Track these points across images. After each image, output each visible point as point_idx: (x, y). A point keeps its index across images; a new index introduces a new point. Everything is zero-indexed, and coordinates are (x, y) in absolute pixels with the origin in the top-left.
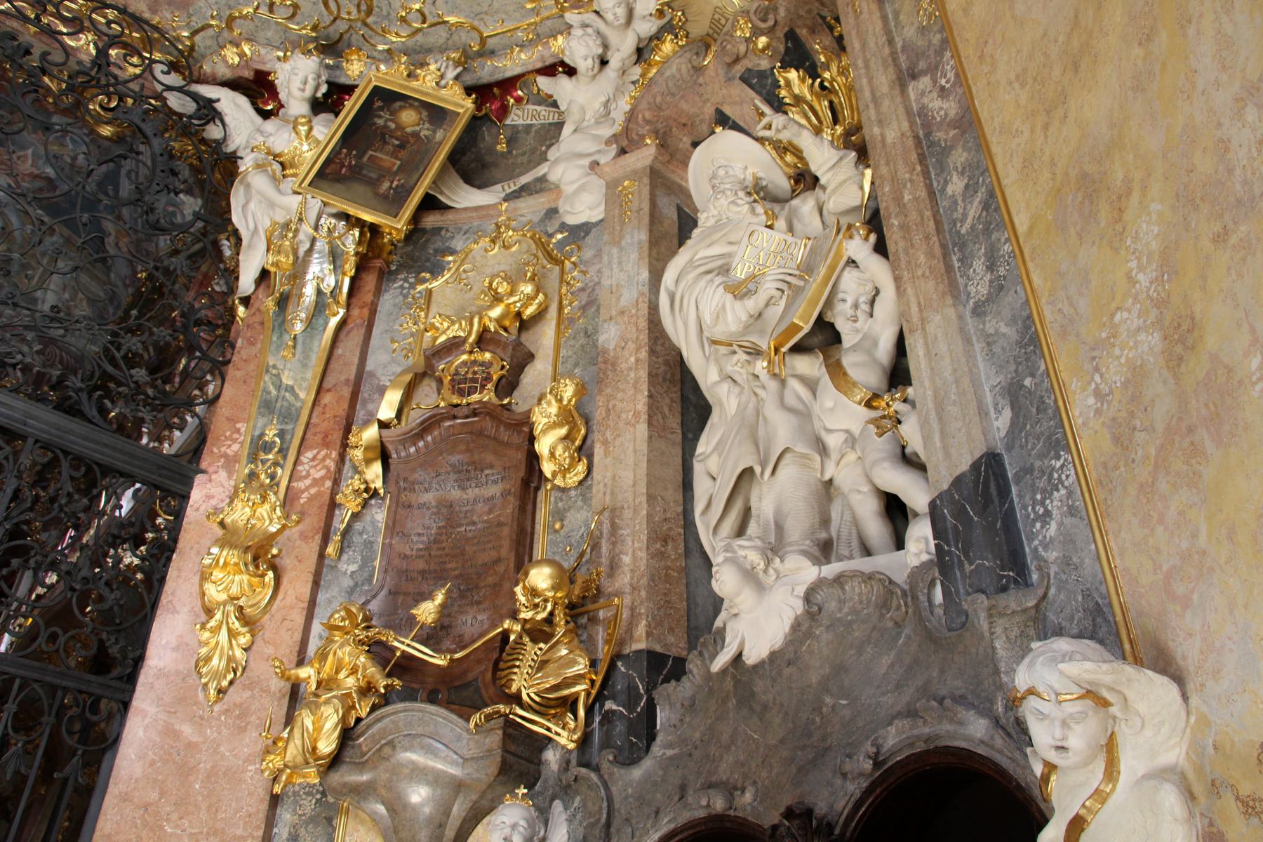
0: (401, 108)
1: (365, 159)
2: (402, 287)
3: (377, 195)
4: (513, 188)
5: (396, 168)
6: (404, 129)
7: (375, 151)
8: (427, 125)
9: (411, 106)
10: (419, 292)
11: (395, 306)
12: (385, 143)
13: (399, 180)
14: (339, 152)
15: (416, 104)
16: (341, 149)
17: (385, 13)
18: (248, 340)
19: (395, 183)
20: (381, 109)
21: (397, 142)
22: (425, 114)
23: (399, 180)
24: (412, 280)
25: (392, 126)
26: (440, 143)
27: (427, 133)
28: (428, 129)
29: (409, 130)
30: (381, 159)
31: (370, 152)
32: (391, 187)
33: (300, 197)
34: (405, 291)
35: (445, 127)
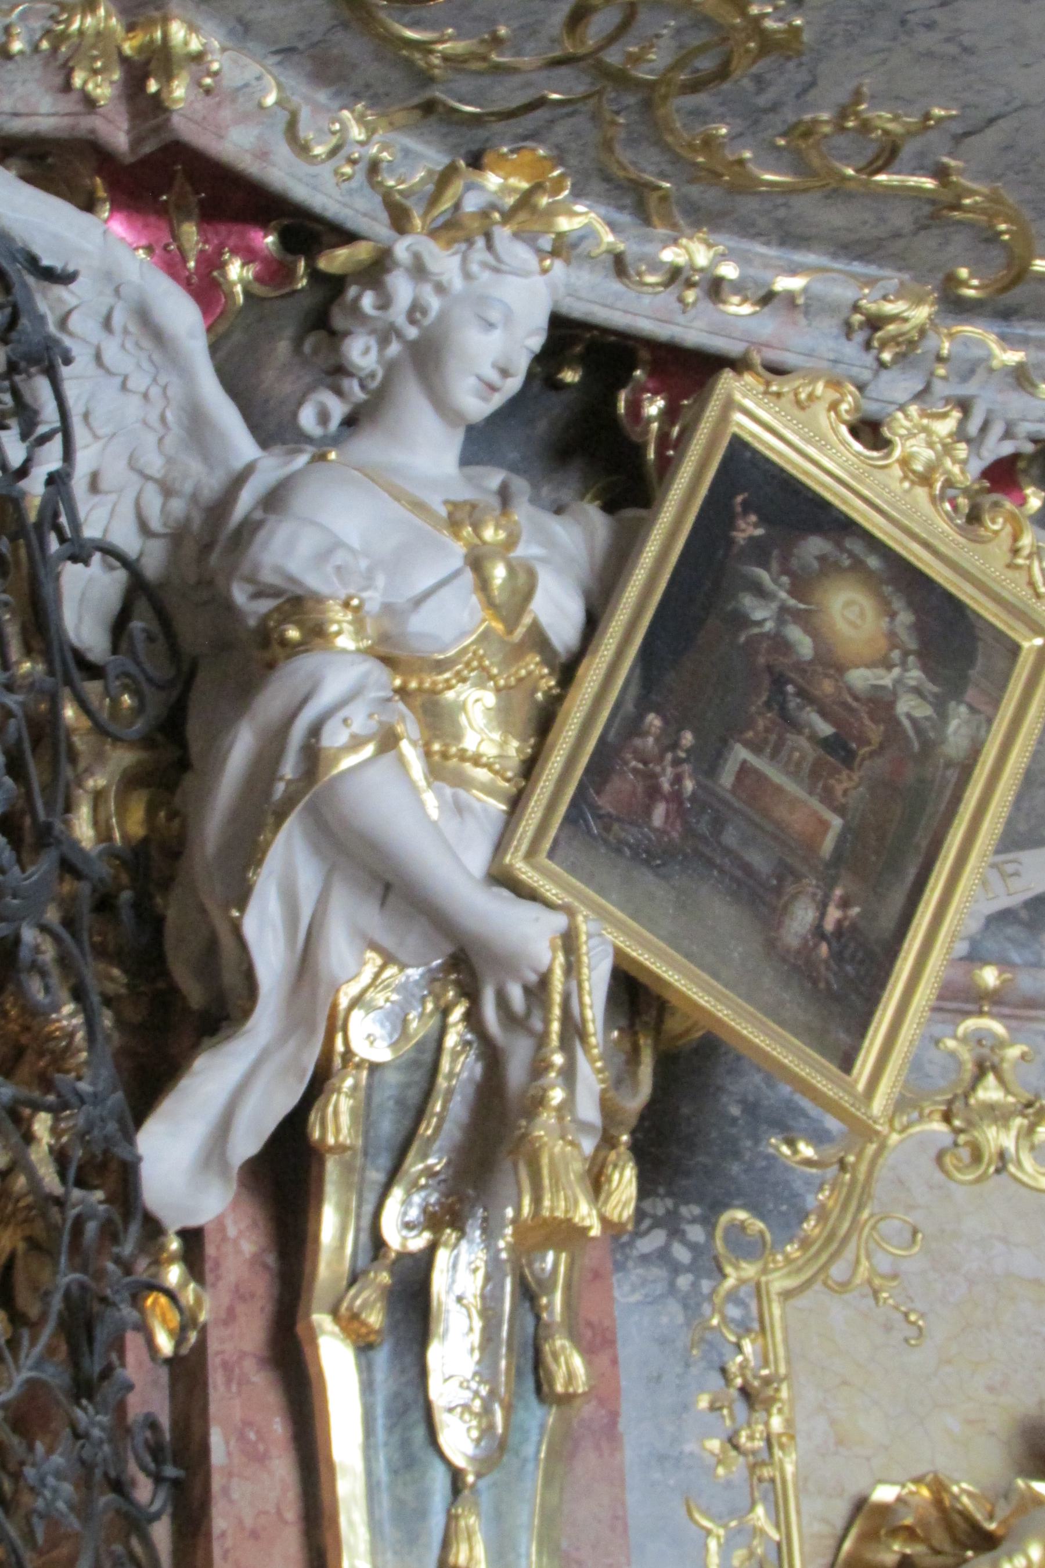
0: (827, 566)
1: (727, 779)
2: (663, 1255)
3: (771, 945)
4: (1004, 902)
5: (828, 845)
6: (841, 669)
7: (757, 748)
8: (915, 675)
9: (858, 565)
10: (732, 1297)
11: (663, 1342)
12: (790, 722)
13: (845, 904)
14: (634, 727)
15: (873, 562)
16: (644, 705)
17: (762, 101)
18: (242, 1437)
19: (834, 914)
20: (759, 552)
21: (825, 729)
22: (905, 617)
23: (845, 904)
24: (696, 1233)
25: (804, 645)
26: (966, 770)
27: (924, 711)
28: (918, 691)
29: (860, 678)
30: (779, 789)
31: (741, 753)
32: (818, 931)
33: (560, 921)
34: (684, 1281)
35: (971, 694)
